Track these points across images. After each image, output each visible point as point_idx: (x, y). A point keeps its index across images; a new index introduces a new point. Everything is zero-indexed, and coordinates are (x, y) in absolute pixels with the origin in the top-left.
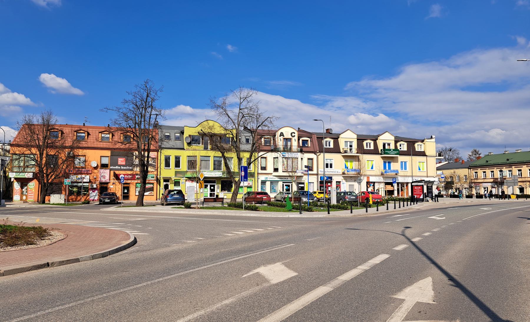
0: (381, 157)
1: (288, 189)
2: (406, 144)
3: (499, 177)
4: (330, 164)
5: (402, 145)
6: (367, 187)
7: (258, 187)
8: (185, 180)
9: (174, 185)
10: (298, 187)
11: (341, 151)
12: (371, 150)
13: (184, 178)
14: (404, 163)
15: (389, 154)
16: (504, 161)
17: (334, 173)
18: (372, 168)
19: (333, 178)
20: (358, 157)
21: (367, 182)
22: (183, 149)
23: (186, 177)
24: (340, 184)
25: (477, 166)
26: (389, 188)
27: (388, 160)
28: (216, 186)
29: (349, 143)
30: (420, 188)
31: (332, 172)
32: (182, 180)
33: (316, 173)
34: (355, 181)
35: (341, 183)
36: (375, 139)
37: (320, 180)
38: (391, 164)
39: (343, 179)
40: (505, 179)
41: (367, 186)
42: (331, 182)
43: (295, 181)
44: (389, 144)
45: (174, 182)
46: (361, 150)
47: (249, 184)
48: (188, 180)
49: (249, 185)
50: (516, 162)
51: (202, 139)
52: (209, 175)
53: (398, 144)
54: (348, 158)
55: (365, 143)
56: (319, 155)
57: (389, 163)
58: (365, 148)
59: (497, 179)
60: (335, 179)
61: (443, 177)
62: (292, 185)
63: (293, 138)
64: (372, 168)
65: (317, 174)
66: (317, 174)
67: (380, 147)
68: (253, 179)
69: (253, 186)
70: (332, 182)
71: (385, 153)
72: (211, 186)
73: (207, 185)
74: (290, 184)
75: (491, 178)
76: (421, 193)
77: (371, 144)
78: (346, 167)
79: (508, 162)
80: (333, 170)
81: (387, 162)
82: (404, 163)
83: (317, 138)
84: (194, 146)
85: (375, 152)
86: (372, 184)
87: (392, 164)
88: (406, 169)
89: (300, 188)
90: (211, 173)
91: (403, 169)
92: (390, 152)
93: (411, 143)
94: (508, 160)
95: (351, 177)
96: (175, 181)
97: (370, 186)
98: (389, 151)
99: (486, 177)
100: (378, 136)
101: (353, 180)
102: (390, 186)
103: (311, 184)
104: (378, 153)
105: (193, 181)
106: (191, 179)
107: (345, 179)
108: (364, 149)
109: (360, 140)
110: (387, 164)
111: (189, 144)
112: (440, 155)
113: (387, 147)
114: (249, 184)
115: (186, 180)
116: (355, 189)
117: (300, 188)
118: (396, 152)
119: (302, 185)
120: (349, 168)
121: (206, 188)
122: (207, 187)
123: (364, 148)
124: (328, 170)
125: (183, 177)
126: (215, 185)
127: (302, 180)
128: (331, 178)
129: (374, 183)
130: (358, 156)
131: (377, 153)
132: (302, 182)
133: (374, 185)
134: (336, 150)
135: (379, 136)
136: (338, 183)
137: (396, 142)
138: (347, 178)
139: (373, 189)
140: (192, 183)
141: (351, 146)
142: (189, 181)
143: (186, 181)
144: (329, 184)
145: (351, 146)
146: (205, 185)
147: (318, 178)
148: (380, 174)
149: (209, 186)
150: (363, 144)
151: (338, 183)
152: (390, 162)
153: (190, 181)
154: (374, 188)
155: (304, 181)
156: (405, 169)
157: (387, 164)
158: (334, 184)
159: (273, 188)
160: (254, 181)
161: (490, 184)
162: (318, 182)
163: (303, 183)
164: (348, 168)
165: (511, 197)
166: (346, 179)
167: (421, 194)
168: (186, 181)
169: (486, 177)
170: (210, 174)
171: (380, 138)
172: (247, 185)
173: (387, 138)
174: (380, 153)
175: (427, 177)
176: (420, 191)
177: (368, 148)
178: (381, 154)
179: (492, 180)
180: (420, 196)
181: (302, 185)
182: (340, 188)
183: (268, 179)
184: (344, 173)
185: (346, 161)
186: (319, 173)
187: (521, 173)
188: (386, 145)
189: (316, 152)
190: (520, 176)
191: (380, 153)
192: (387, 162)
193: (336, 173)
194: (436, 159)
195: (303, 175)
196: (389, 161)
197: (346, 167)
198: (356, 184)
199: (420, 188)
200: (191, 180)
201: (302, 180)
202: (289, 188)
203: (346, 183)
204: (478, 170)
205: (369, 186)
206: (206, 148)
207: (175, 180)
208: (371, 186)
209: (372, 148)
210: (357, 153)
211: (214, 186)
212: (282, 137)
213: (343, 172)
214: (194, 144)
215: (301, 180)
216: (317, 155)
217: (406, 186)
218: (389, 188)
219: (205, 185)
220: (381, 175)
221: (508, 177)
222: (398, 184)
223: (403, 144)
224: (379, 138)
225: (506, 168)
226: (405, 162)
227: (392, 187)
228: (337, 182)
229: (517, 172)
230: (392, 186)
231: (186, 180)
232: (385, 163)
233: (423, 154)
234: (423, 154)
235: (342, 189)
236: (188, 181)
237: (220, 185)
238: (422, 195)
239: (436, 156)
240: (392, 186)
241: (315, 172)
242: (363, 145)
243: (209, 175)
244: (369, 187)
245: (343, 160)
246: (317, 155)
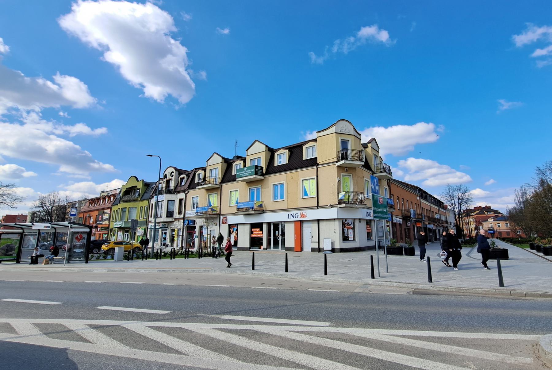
14: (279, 185)
26: (257, 233)
82: (279, 185)
86: (236, 228)
88: (283, 198)
91: (278, 199)
92: (243, 172)
97: (233, 232)
98: (241, 173)
102: (258, 230)
118: (251, 171)
128: (194, 222)
133: (237, 230)
136: (201, 227)
139: (236, 236)
154: (237, 234)
156: (281, 198)
158: (197, 230)
175: (318, 208)
192: (255, 189)
205: (232, 231)
208: (234, 231)
212: (166, 179)
226: (282, 185)
233: (313, 162)
234: (313, 162)
240: (261, 230)
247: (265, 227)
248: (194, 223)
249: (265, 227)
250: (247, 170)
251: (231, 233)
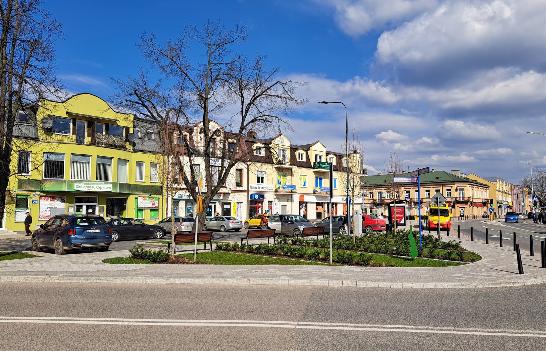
0: (313, 171)
1: (210, 211)
2: (335, 157)
3: (415, 197)
4: (262, 177)
5: (331, 158)
6: (300, 209)
7: (167, 210)
8: (38, 197)
9: (15, 205)
10: (223, 209)
11: (275, 161)
12: (303, 162)
13: (38, 193)
15: (323, 168)
16: (381, 182)
17: (266, 190)
18: (304, 185)
19: (266, 196)
20: (292, 170)
21: (300, 202)
22: (37, 139)
23: (40, 192)
24: (272, 205)
25: (382, 186)
26: (320, 209)
27: (319, 176)
28: (97, 209)
29: (281, 151)
30: (400, 210)
31: (264, 188)
32: (33, 196)
33: (246, 189)
34: (288, 201)
35: (273, 203)
36: (307, 148)
37: (251, 198)
38: (322, 180)
39: (275, 197)
40: (384, 200)
41: (300, 207)
42: (262, 202)
43: (219, 201)
44: (320, 157)
45: (15, 199)
46: (294, 161)
47: (154, 204)
48: (45, 197)
49: (154, 206)
50: (447, 181)
51: (74, 125)
52: (89, 189)
53: (329, 156)
54: (282, 171)
55: (297, 153)
56: (249, 165)
57: (321, 179)
58: (298, 160)
59: (376, 200)
60: (269, 197)
61: (407, 196)
62: (215, 205)
63: (218, 137)
64: (304, 185)
65: (247, 191)
66: (247, 191)
67: (313, 160)
68: (161, 197)
69: (160, 207)
70: (263, 201)
71: (319, 167)
72: (88, 208)
73: (82, 206)
74: (213, 205)
75: (370, 200)
76: (402, 216)
77: (303, 154)
78: (279, 183)
79: (437, 181)
80: (265, 186)
81: (319, 178)
83: (247, 141)
84: (58, 137)
85: (307, 165)
86: (304, 205)
87: (323, 180)
89: (225, 210)
90: (91, 186)
93: (339, 157)
94: (437, 178)
95: (284, 195)
96: (19, 197)
97: (302, 207)
99: (372, 197)
100: (311, 146)
101: (286, 199)
102: (321, 207)
103: (239, 204)
104: (310, 167)
105: (53, 198)
106: (52, 195)
107: (277, 198)
108: (297, 161)
109: (294, 149)
110: (319, 180)
111: (49, 131)
112: (364, 172)
113: (318, 160)
114: (154, 204)
115: (41, 197)
116: (288, 211)
117: (225, 210)
119: (228, 207)
120: (281, 184)
121: (80, 211)
122: (81, 210)
123: (296, 160)
124: (260, 186)
125: (35, 191)
126: (95, 206)
127: (229, 199)
128: (263, 196)
129: (306, 203)
130: (291, 169)
131: (311, 168)
132: (228, 201)
133: (306, 206)
134: (268, 160)
135: (311, 146)
137: (327, 154)
138: (281, 196)
139: (305, 211)
140: (52, 202)
141: (284, 156)
142: (46, 198)
143: (40, 199)
144: (260, 205)
145: (284, 156)
146: (76, 205)
147: (248, 196)
148: (312, 193)
149: (84, 208)
150: (295, 154)
151: (270, 202)
152: (321, 178)
153: (48, 199)
154: (306, 210)
155: (231, 200)
157: (319, 180)
159: (188, 211)
160: (161, 200)
161: (369, 205)
162: (247, 201)
163: (229, 204)
164: (280, 184)
165: (415, 218)
166: (279, 198)
167: (403, 218)
168: (40, 199)
169: (372, 197)
170: (90, 187)
171: (313, 148)
172: (150, 206)
173: (318, 149)
174: (313, 166)
176: (401, 214)
177: (300, 160)
178: (314, 168)
179: (371, 201)
180: (401, 220)
181: (228, 207)
182: (272, 210)
183: (183, 198)
184: (276, 191)
185: (279, 175)
186: (250, 189)
187: (450, 193)
188: (318, 157)
189: (246, 161)
190: (449, 196)
191: (313, 166)
192: (319, 178)
193: (269, 190)
194: (361, 177)
195: (230, 192)
196: (321, 176)
197: (279, 183)
198: (289, 204)
199: (400, 210)
200: (50, 197)
201: (229, 199)
202: (211, 210)
203: (278, 203)
204: (382, 190)
205: (301, 207)
206: (80, 141)
207: (17, 195)
208: (303, 207)
209: (304, 160)
210: (291, 165)
211: (93, 208)
213: (276, 189)
214: (57, 132)
215: (227, 199)
216: (247, 165)
217: (335, 206)
218: (320, 209)
219: (76, 205)
220: (314, 193)
221: (386, 198)
222: (328, 204)
223: (332, 158)
224: (311, 148)
225: (384, 189)
227: (323, 209)
228: (269, 201)
229: (378, 194)
230: (323, 207)
231: (41, 197)
232: (317, 178)
235: (274, 210)
236: (44, 199)
237: (105, 207)
238: (404, 219)
239: (360, 173)
241: (244, 188)
242: (295, 156)
243: (89, 189)
244: (301, 207)
245: (276, 173)
246: (247, 165)
247: (326, 206)
248: (264, 198)
249: (326, 206)
250: (327, 165)
251: (301, 209)
